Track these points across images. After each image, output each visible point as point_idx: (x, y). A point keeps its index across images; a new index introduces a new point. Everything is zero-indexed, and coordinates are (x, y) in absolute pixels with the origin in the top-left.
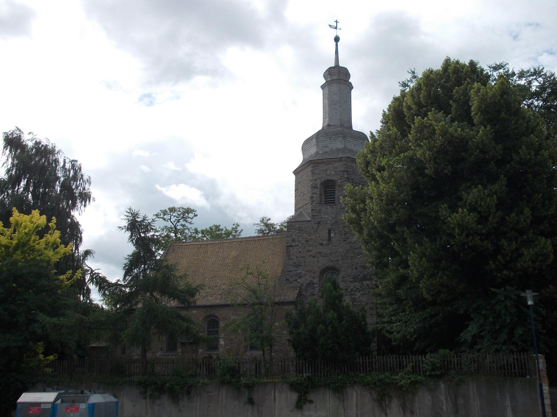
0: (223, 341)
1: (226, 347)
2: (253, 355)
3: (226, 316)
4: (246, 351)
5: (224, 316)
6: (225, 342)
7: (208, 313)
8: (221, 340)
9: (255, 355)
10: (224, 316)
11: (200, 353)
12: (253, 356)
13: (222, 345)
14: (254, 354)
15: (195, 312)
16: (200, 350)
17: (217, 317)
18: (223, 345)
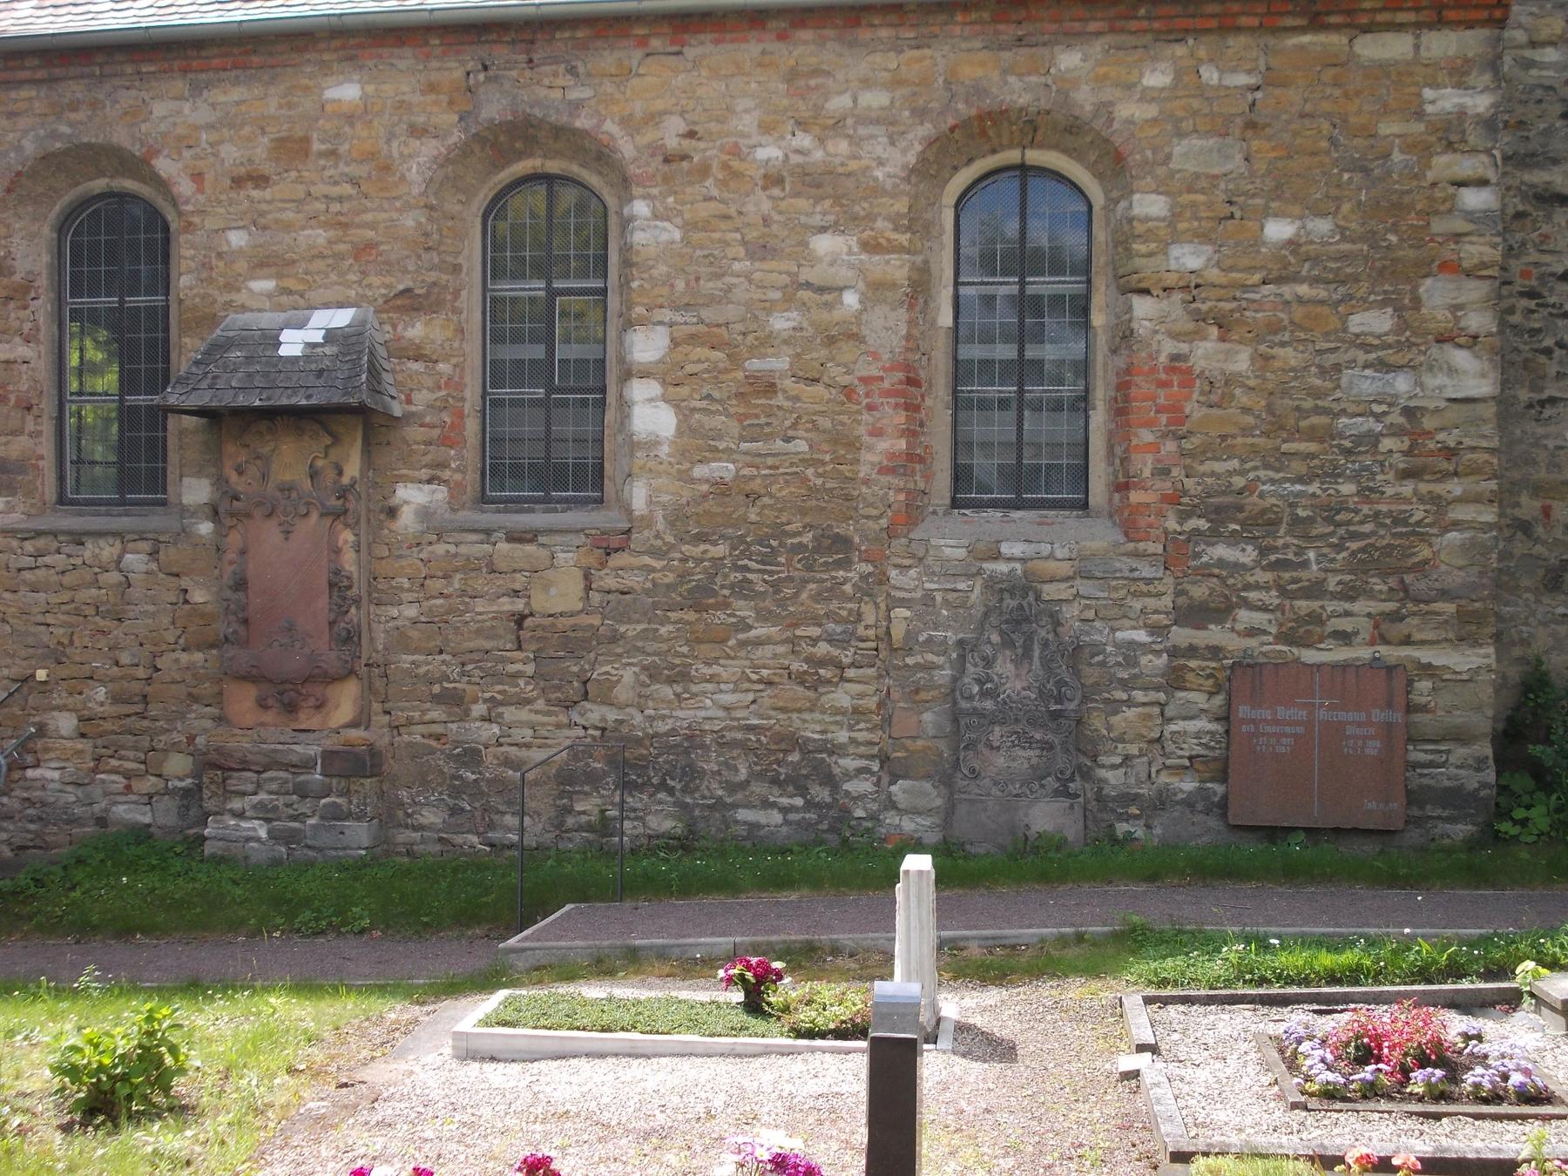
0: (665, 399)
1: (699, 471)
2: (997, 556)
3: (691, 134)
4: (913, 512)
5: (672, 143)
6: (684, 414)
7: (494, 108)
8: (641, 391)
9: (1023, 560)
10: (671, 133)
11: (407, 520)
12: (1002, 567)
13: (654, 443)
14: (1005, 548)
15: (346, 91)
16: (413, 497)
17: (602, 157)
18: (664, 450)
